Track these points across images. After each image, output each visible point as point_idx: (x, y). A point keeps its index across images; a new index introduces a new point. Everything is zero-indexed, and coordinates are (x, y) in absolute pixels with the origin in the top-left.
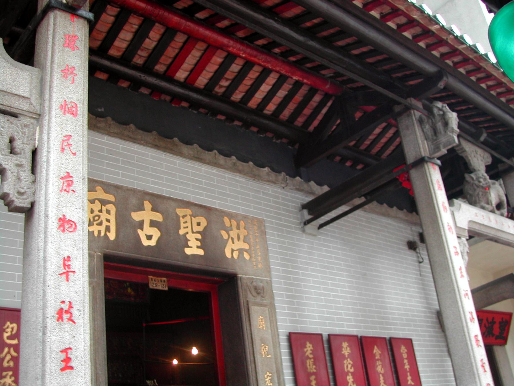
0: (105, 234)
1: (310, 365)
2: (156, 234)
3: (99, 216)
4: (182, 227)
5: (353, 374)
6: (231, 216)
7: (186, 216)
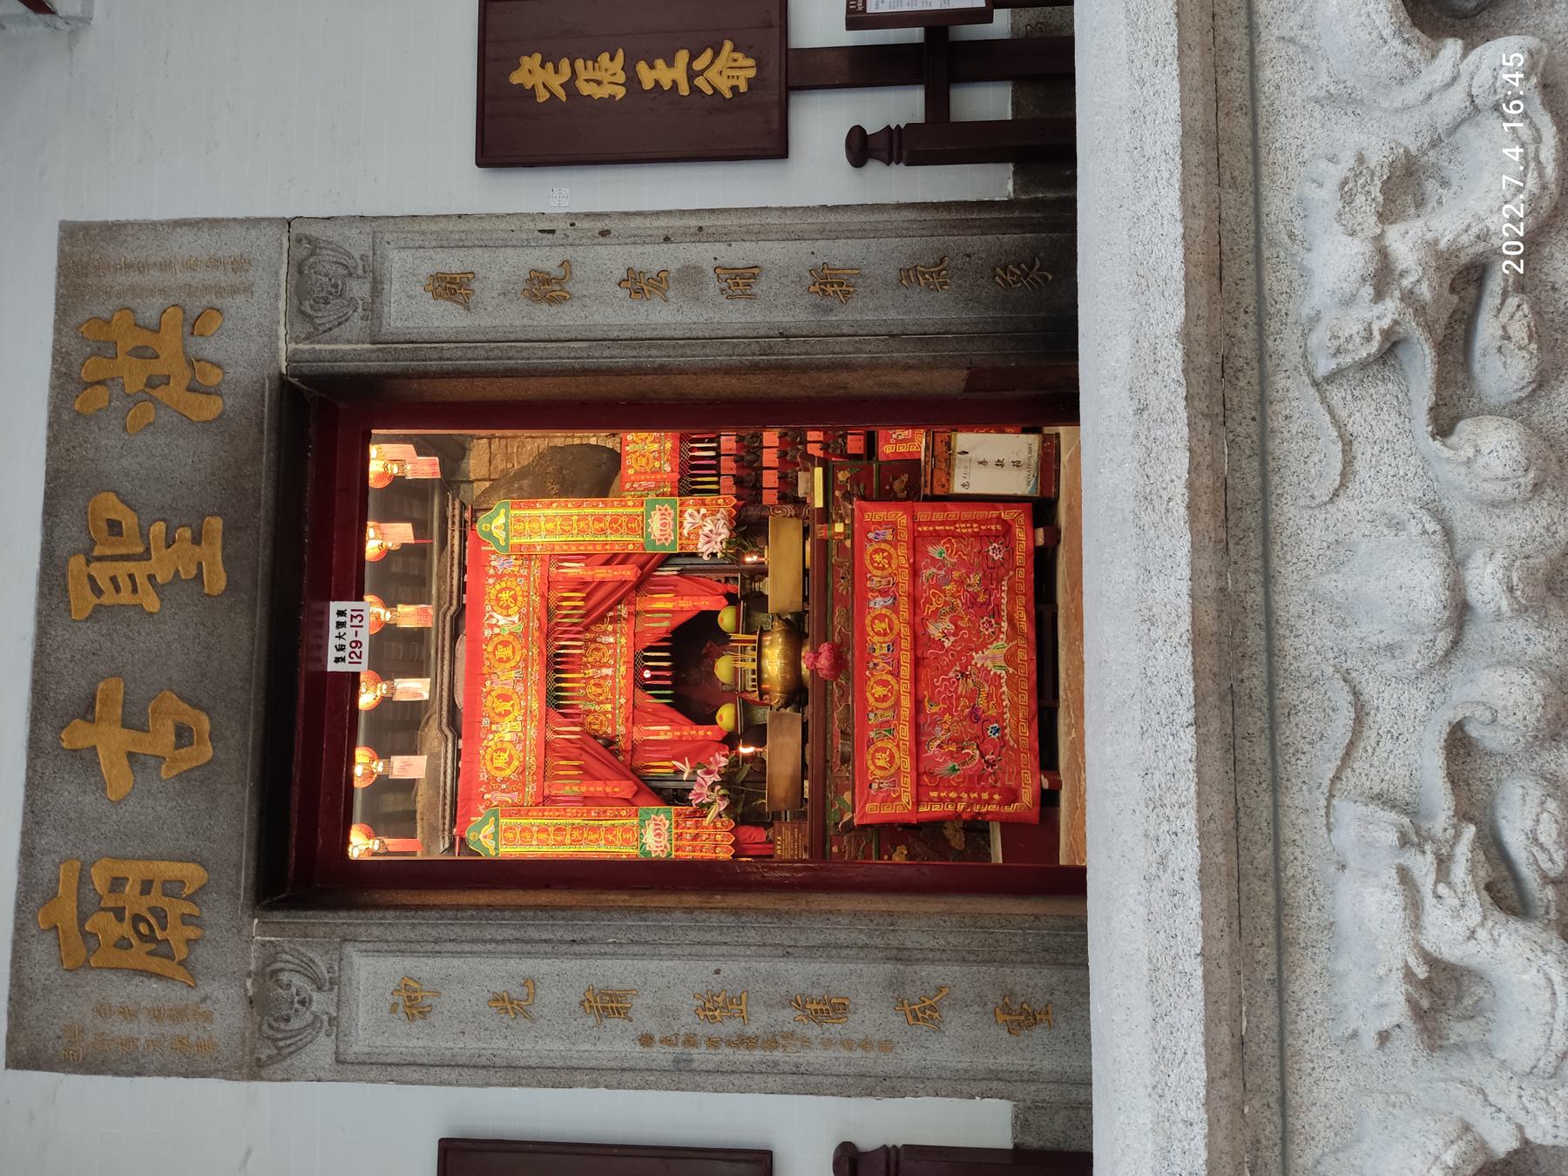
0: (190, 898)
1: (599, 83)
3: (137, 919)
4: (134, 600)
7: (92, 579)
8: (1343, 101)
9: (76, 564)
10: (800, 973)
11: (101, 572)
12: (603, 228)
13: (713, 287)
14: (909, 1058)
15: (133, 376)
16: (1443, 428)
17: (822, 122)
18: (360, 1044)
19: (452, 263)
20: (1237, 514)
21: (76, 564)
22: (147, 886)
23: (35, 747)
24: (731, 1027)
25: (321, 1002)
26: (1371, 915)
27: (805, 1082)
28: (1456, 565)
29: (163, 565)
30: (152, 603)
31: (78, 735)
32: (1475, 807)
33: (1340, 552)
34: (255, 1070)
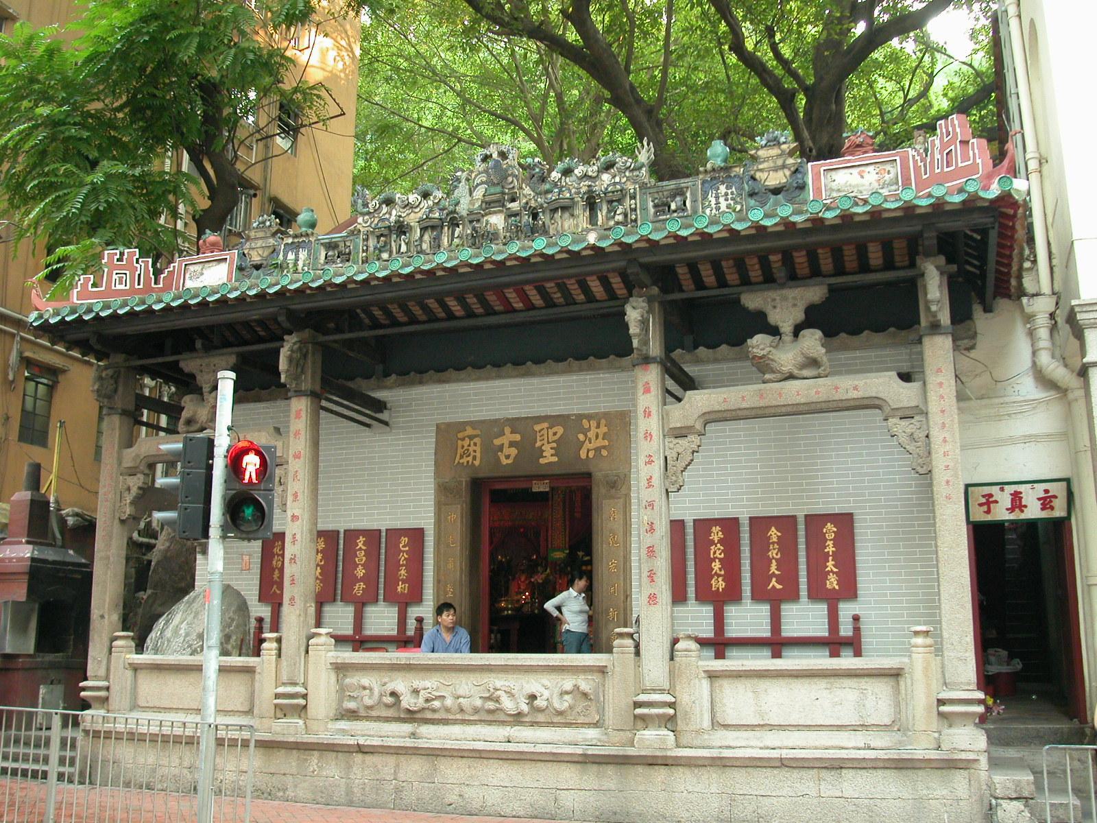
2: (513, 452)
5: (720, 560)
6: (589, 417)
11: (545, 432)
22: (475, 451)
31: (507, 430)
32: (437, 698)
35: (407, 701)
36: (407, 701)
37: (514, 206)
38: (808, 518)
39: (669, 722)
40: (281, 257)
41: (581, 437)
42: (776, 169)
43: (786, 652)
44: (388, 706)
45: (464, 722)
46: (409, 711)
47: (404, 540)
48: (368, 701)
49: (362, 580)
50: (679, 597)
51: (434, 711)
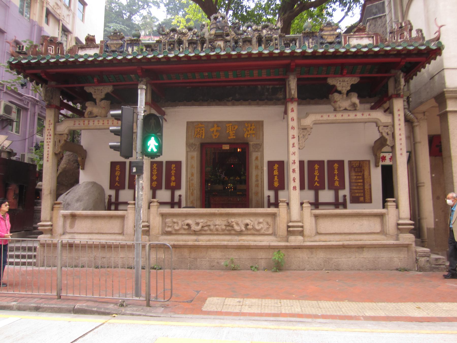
2: (218, 134)
8: (242, 221)
9: (231, 124)
10: (195, 192)
12: (262, 173)
13: (256, 183)
14: (188, 201)
15: (249, 129)
16: (225, 225)
17: (271, 194)
18: (189, 153)
19: (259, 158)
20: (221, 215)
21: (231, 124)
23: (214, 122)
24: (191, 185)
25: (192, 149)
26: (201, 221)
27: (186, 192)
28: (218, 225)
29: (231, 133)
30: (227, 132)
31: (215, 126)
32: (207, 226)
33: (219, 220)
34: (187, 144)
35: (194, 227)
36: (194, 227)
37: (228, 38)
38: (329, 162)
39: (301, 233)
40: (125, 48)
41: (245, 130)
42: (331, 35)
43: (320, 207)
44: (184, 229)
45: (217, 234)
46: (194, 231)
47: (173, 166)
48: (177, 228)
49: (155, 180)
50: (302, 187)
51: (205, 231)
